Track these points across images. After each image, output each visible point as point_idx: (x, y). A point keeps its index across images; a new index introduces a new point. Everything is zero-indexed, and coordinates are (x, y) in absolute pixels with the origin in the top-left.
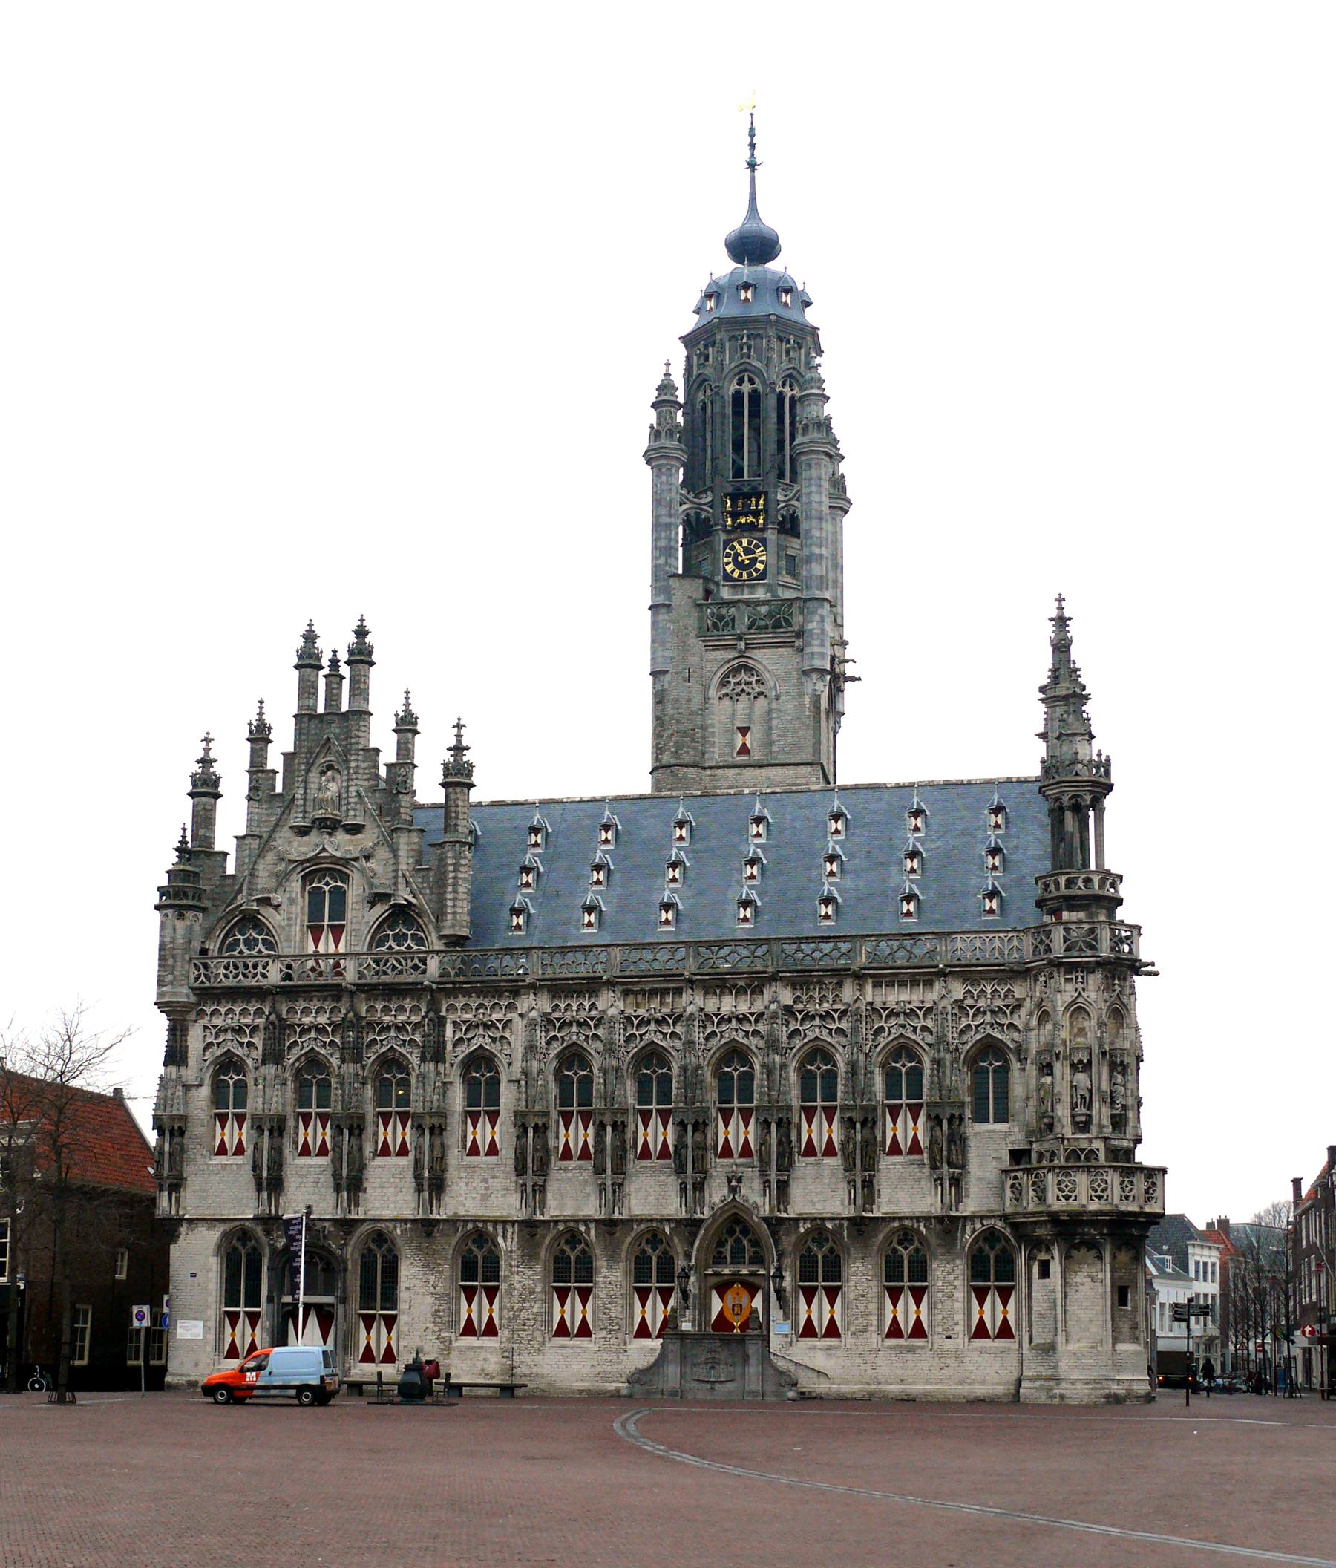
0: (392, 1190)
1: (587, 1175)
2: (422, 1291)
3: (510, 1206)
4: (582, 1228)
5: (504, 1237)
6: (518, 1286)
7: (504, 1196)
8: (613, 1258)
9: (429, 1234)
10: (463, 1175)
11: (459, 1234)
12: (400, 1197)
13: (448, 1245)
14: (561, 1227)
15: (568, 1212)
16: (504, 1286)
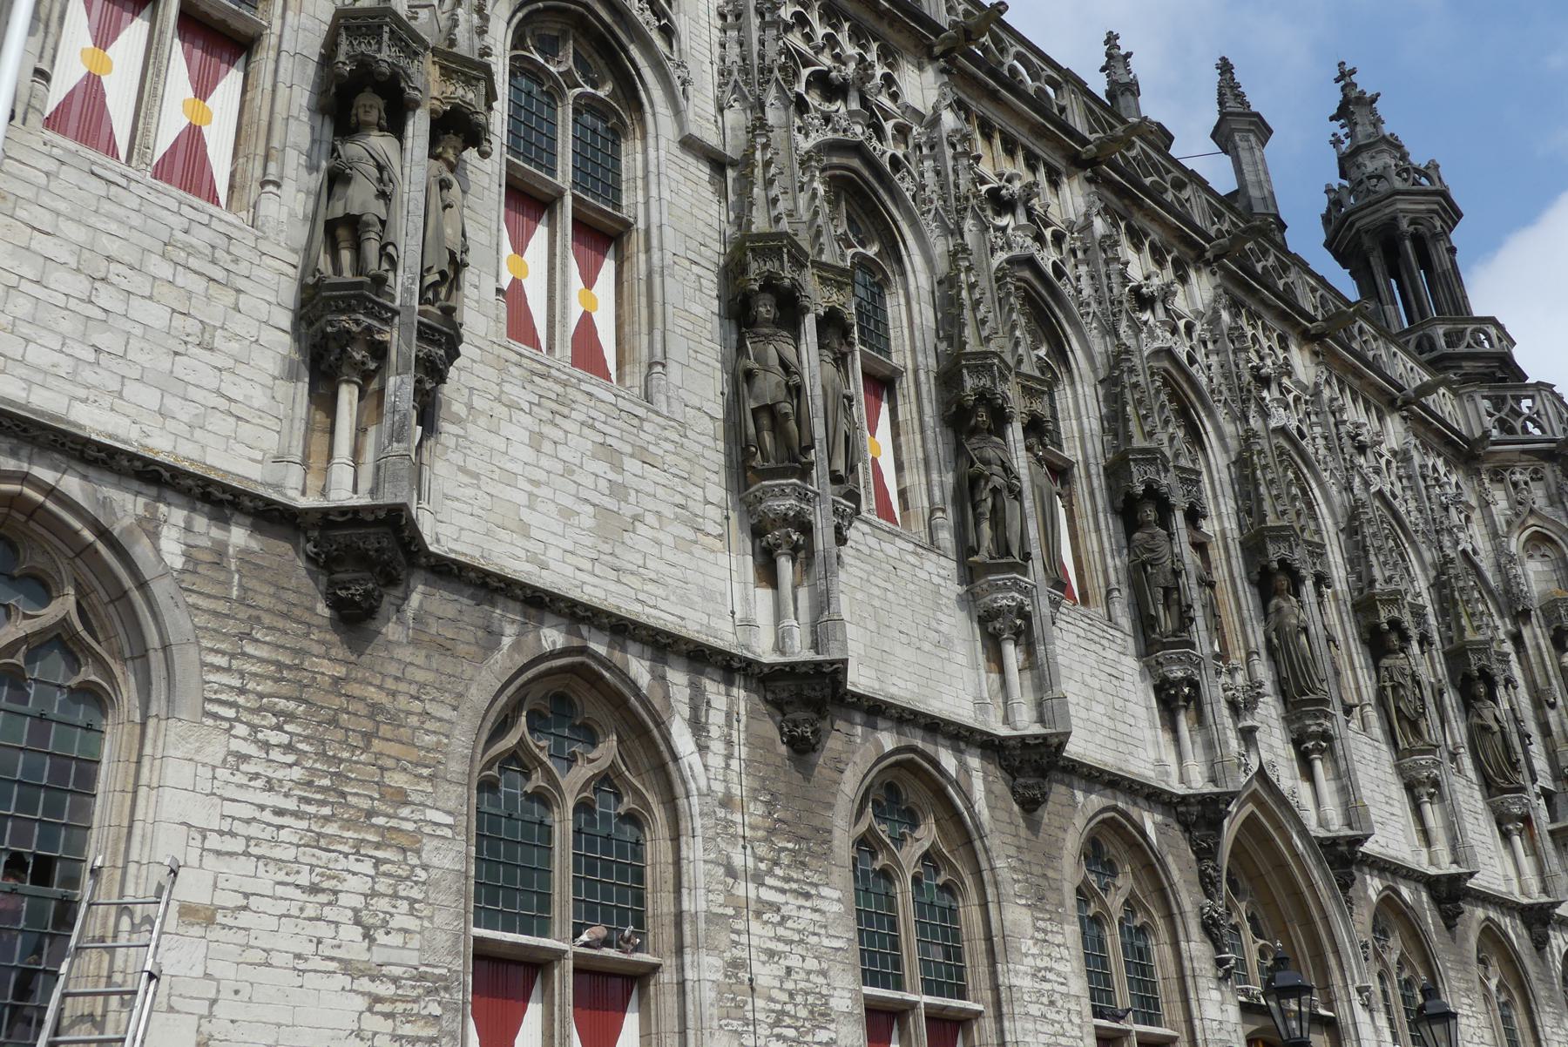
0: (155, 315)
1: (941, 571)
2: (290, 940)
3: (708, 595)
4: (948, 761)
5: (698, 726)
6: (766, 975)
7: (680, 544)
8: (1039, 899)
9: (354, 618)
10: (514, 391)
11: (505, 659)
12: (197, 366)
13: (444, 687)
14: (888, 740)
15: (899, 689)
16: (706, 970)
